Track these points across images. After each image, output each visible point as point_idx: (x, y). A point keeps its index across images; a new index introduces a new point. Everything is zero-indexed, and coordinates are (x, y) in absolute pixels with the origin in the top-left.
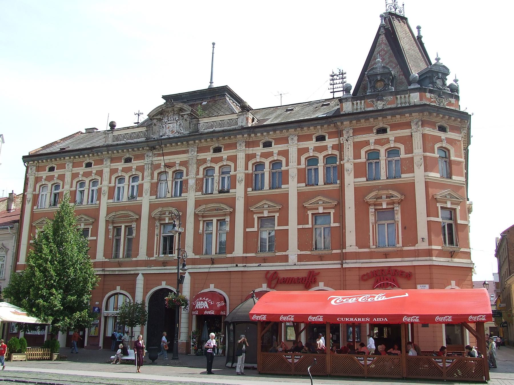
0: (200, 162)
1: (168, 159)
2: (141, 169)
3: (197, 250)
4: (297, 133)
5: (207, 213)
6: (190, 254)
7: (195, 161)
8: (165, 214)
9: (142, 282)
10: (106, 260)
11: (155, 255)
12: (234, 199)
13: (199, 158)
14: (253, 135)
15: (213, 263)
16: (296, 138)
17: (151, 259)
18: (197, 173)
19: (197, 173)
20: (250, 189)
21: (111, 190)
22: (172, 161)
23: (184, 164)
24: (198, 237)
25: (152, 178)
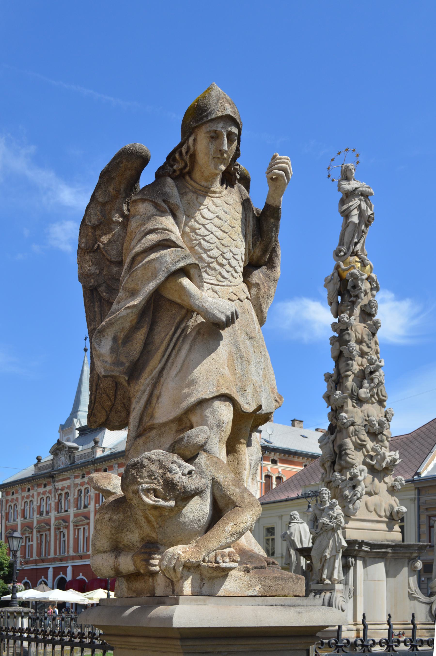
0: (76, 485)
1: (59, 485)
2: (50, 492)
3: (76, 549)
4: (116, 462)
5: (78, 524)
6: (72, 553)
7: (72, 485)
8: (61, 525)
9: (52, 573)
10: (37, 558)
11: (58, 554)
12: (89, 513)
13: (75, 483)
14: (96, 465)
15: (81, 559)
16: (116, 466)
17: (56, 556)
18: (74, 495)
19: (74, 495)
20: (97, 505)
21: (39, 507)
22: (64, 485)
23: (69, 487)
24: (76, 541)
25: (55, 499)
